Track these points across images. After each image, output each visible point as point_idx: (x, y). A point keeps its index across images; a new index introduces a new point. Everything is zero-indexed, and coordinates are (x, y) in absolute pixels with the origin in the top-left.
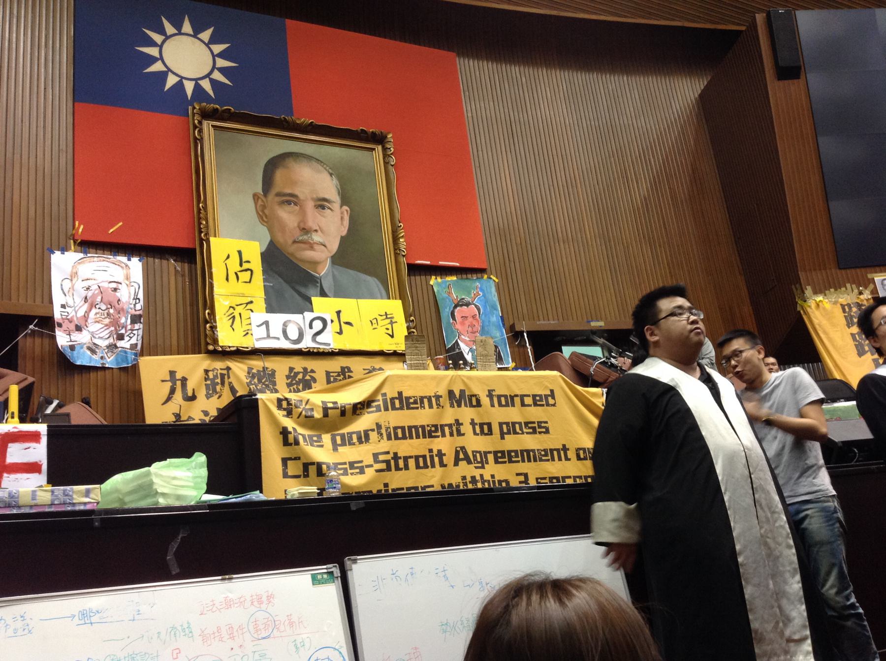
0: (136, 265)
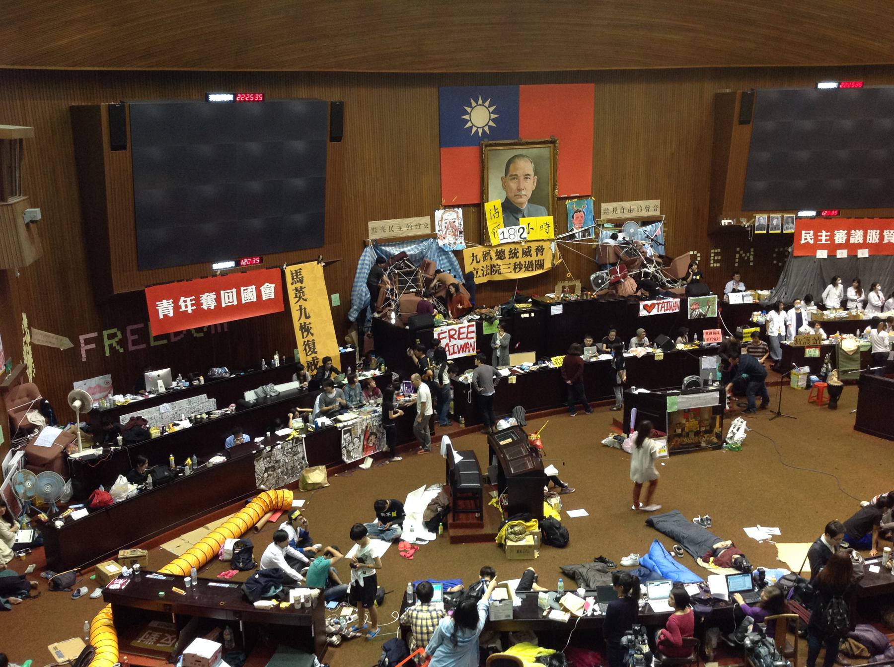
0: (460, 211)
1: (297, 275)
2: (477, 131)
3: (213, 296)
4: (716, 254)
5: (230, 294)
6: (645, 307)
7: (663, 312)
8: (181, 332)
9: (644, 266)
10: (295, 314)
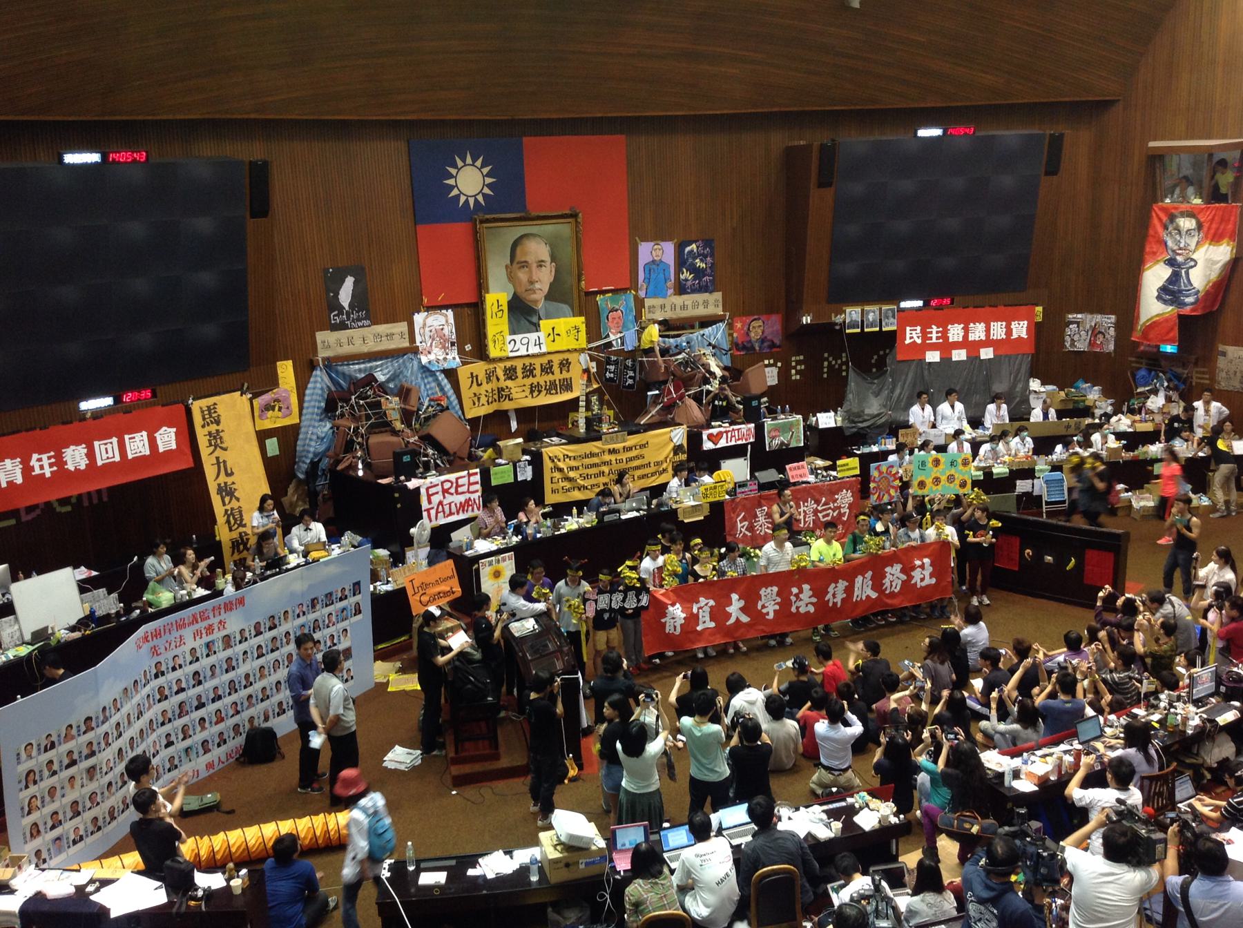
0: (450, 313)
1: (210, 414)
2: (467, 201)
3: (81, 450)
4: (798, 363)
5: (109, 446)
6: (710, 437)
7: (733, 443)
8: (37, 506)
9: (706, 381)
10: (210, 471)
